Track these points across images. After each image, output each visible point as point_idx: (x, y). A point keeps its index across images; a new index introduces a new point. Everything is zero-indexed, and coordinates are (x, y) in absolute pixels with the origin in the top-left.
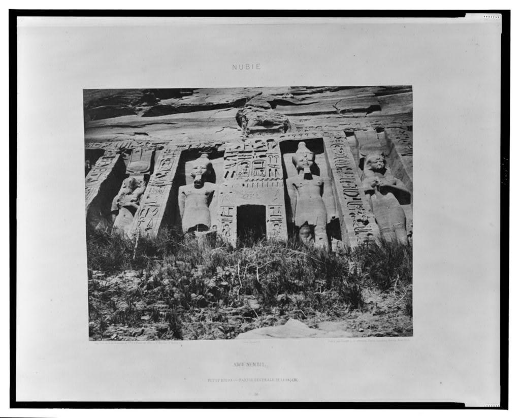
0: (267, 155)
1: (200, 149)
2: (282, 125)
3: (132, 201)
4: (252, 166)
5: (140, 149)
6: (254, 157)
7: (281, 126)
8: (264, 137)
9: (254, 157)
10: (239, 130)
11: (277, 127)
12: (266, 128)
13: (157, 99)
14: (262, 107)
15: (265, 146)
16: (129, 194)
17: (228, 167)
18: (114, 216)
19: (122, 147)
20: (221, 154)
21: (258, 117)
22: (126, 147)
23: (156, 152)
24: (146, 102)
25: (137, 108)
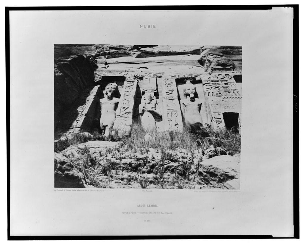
0: (229, 83)
2: (232, 66)
3: (152, 108)
4: (222, 90)
7: (231, 66)
8: (223, 73)
9: (221, 84)
10: (202, 68)
11: (229, 67)
12: (223, 68)
13: (139, 48)
15: (225, 78)
16: (149, 103)
17: (208, 89)
18: (141, 116)
19: (135, 75)
20: (200, 82)
21: (218, 61)
22: (138, 76)
23: (157, 79)
24: (136, 49)
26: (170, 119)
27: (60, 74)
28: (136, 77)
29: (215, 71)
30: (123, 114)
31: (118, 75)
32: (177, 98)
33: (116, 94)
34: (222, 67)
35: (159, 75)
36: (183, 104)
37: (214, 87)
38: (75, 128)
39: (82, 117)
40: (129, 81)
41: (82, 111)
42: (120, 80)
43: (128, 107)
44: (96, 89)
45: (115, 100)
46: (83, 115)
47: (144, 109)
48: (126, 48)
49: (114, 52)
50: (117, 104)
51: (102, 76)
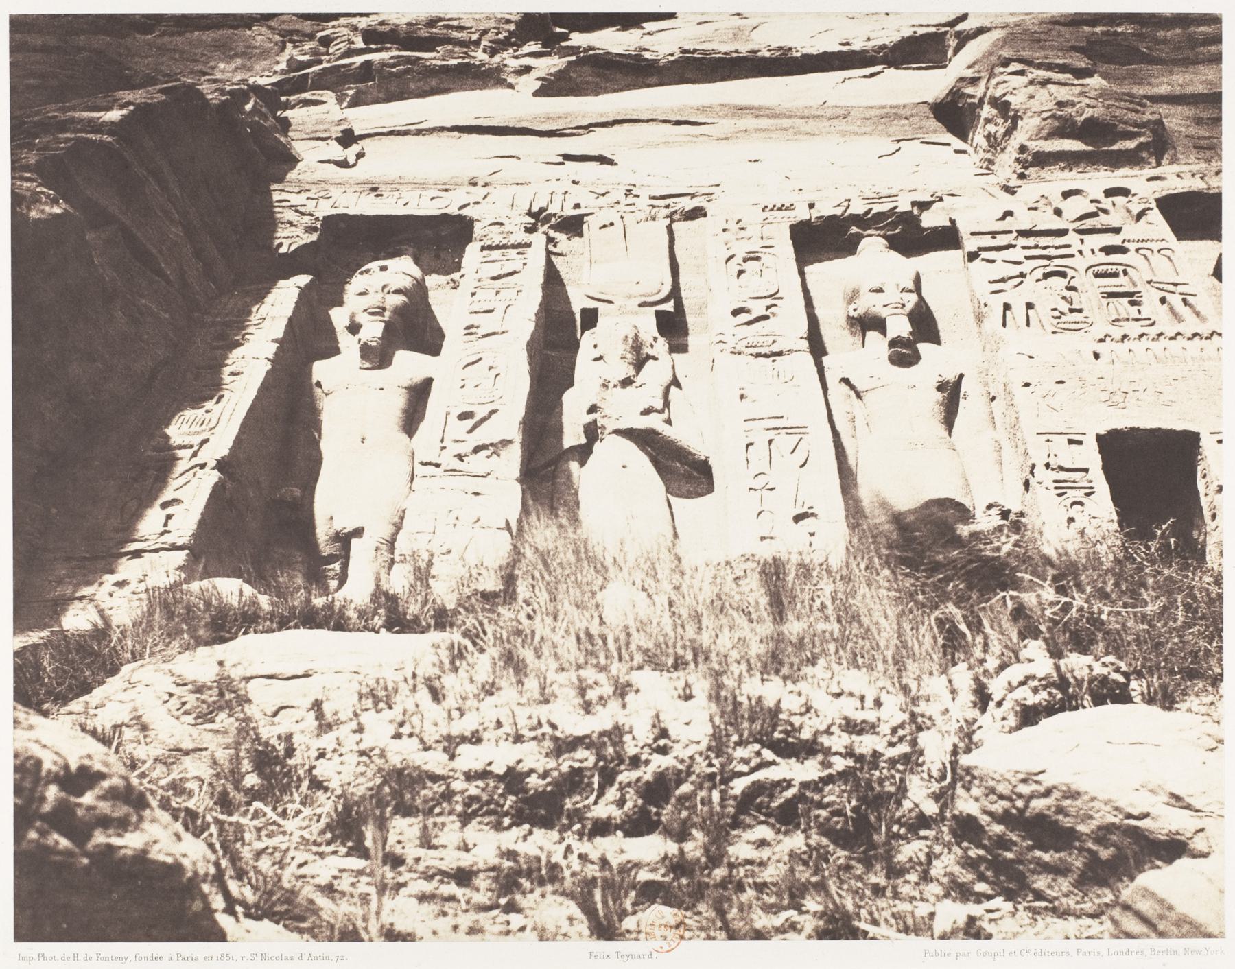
1: (858, 220)
3: (647, 412)
4: (1090, 290)
5: (613, 215)
6: (1080, 252)
7: (1142, 139)
8: (1096, 181)
9: (1080, 252)
10: (957, 152)
11: (1131, 145)
12: (1090, 148)
13: (558, 30)
14: (1063, 69)
15: (1105, 212)
16: (626, 382)
18: (574, 465)
19: (535, 209)
20: (947, 238)
21: (1061, 104)
23: (674, 225)
24: (536, 39)
25: (513, 64)
26: (761, 481)
28: (538, 217)
29: (1043, 173)
30: (460, 457)
31: (424, 206)
32: (806, 344)
33: (414, 327)
34: (1086, 144)
35: (688, 204)
36: (846, 381)
37: (1039, 274)
38: (156, 551)
39: (195, 481)
40: (498, 247)
41: (196, 441)
42: (440, 240)
43: (493, 412)
44: (284, 298)
45: (410, 364)
46: (203, 466)
47: (595, 421)
48: (475, 37)
49: (394, 66)
50: (419, 394)
51: (321, 215)
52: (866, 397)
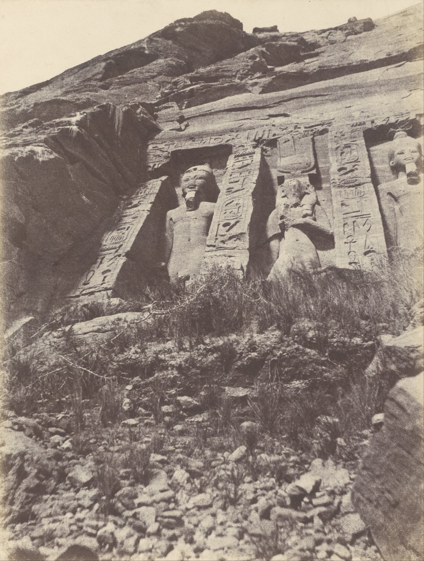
3: (305, 216)
5: (289, 137)
13: (269, 67)
16: (296, 205)
19: (257, 138)
22: (265, 137)
23: (315, 138)
24: (259, 72)
25: (250, 82)
26: (350, 239)
27: (52, 157)
28: (258, 142)
30: (223, 242)
31: (211, 142)
32: (370, 179)
33: (209, 191)
35: (320, 128)
36: (390, 194)
38: (100, 291)
39: (116, 262)
40: (241, 155)
41: (118, 245)
42: (218, 155)
43: (238, 222)
44: (155, 185)
45: (205, 206)
46: (119, 256)
47: (283, 222)
48: (234, 74)
49: (202, 90)
50: (209, 218)
51: (170, 151)
52: (400, 200)
